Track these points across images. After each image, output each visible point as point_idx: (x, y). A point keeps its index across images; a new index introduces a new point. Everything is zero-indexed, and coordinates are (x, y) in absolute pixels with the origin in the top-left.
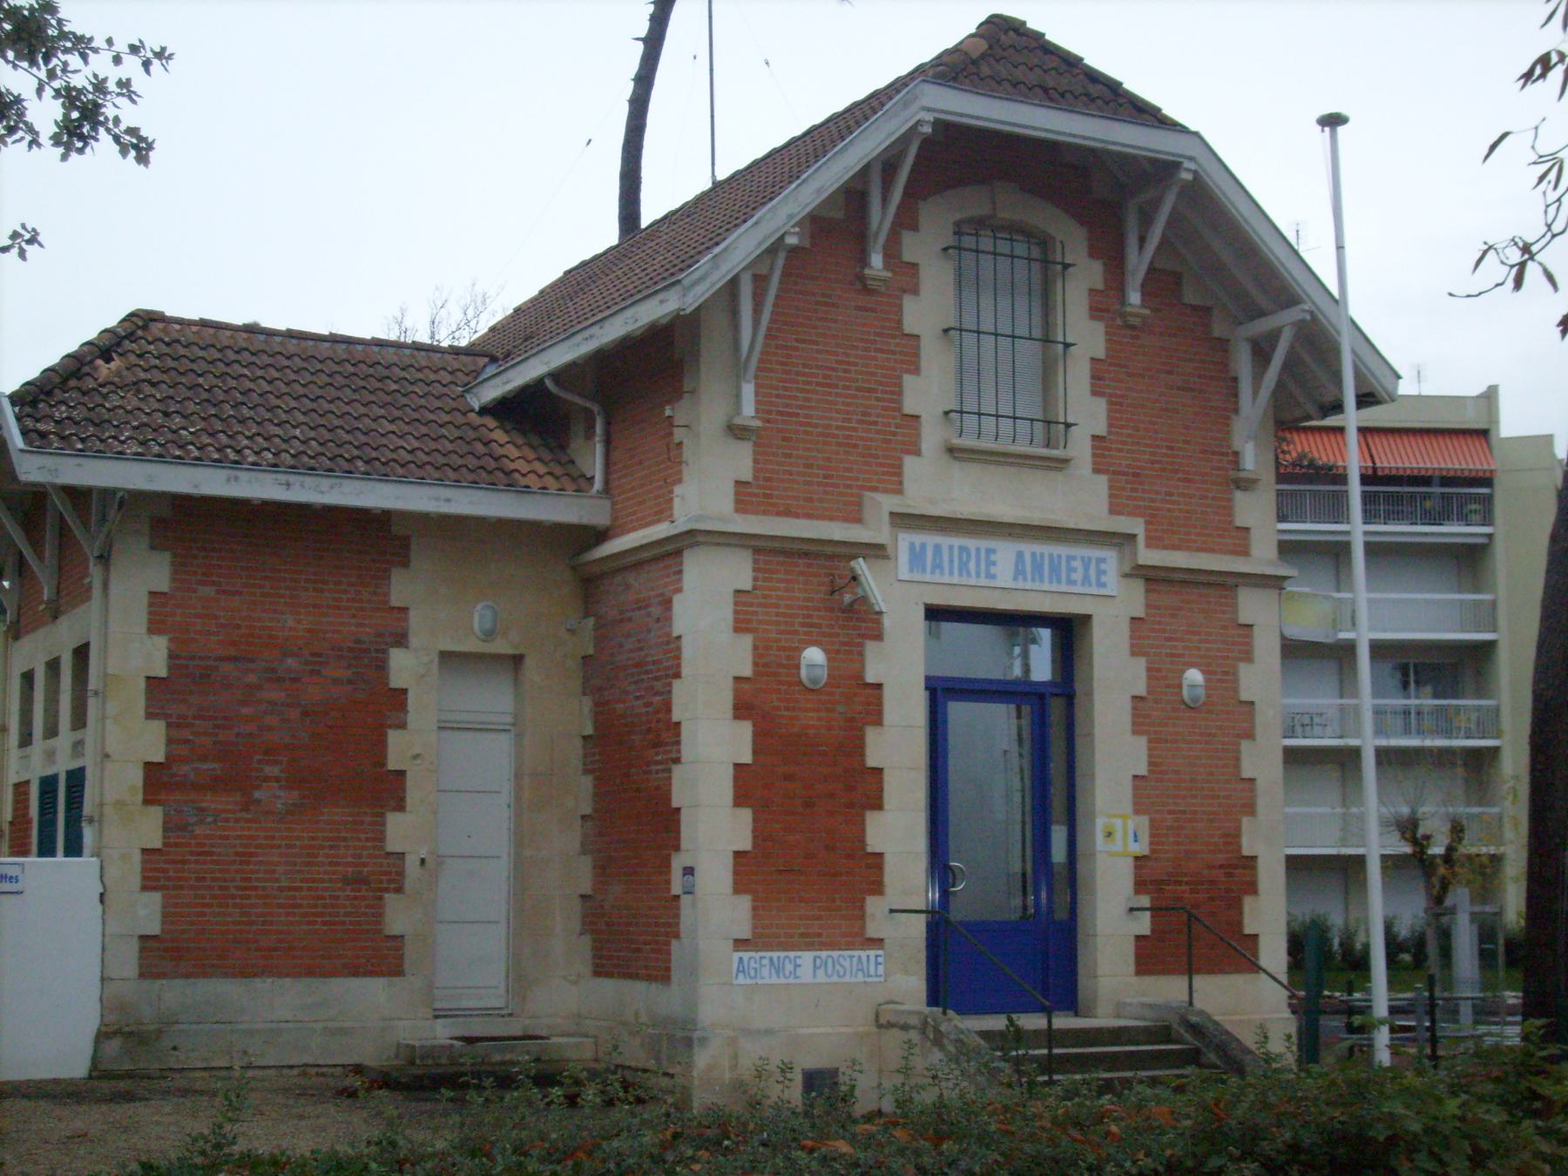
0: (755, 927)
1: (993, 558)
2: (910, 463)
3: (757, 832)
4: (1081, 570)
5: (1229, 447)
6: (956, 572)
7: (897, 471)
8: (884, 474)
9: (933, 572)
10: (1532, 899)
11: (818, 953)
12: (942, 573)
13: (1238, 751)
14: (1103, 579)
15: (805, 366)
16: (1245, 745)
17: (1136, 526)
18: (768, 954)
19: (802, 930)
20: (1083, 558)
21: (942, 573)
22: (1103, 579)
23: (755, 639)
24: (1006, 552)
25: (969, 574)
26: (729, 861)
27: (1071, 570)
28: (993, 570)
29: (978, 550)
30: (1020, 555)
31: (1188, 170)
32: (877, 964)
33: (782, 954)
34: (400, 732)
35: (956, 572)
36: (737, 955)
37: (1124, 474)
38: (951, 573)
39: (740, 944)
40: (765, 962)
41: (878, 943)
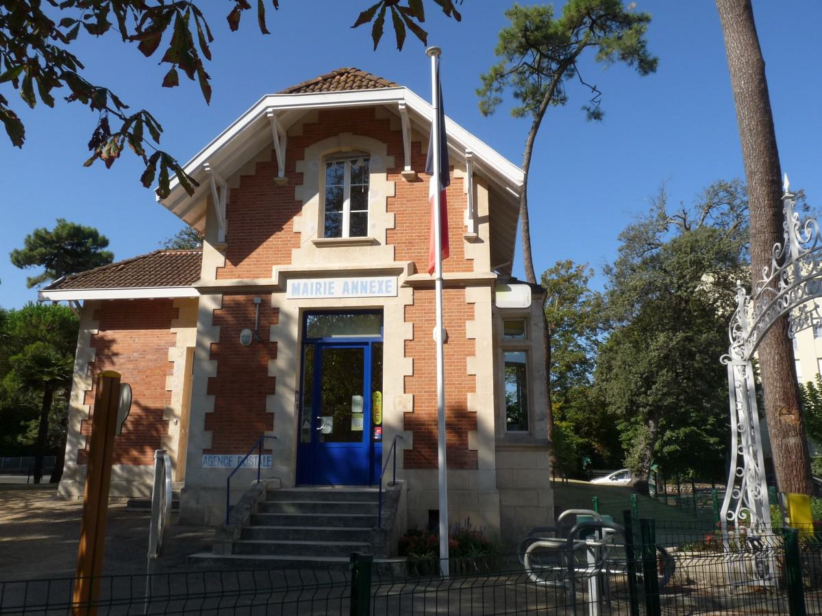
0: (213, 443)
1: (332, 285)
2: (295, 252)
3: (216, 405)
4: (377, 287)
5: (463, 224)
6: (314, 293)
7: (289, 255)
8: (284, 257)
9: (303, 294)
10: (21, 473)
11: (240, 455)
12: (307, 294)
13: (465, 362)
14: (389, 289)
15: (251, 220)
16: (469, 359)
17: (404, 264)
18: (218, 456)
19: (235, 446)
20: (379, 281)
21: (348, 293)
22: (389, 289)
23: (221, 328)
24: (338, 282)
25: (320, 294)
26: (203, 417)
27: (372, 287)
28: (332, 290)
29: (325, 283)
30: (346, 283)
31: (402, 105)
32: (268, 461)
33: (224, 456)
34: (471, 357)
35: (314, 293)
36: (204, 456)
37: (404, 243)
38: (312, 293)
39: (206, 451)
40: (217, 459)
41: (269, 452)
